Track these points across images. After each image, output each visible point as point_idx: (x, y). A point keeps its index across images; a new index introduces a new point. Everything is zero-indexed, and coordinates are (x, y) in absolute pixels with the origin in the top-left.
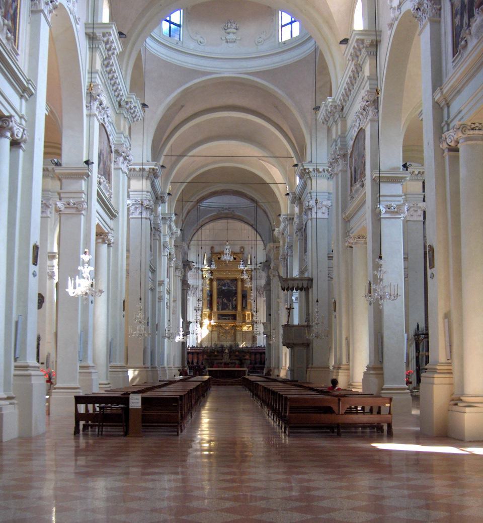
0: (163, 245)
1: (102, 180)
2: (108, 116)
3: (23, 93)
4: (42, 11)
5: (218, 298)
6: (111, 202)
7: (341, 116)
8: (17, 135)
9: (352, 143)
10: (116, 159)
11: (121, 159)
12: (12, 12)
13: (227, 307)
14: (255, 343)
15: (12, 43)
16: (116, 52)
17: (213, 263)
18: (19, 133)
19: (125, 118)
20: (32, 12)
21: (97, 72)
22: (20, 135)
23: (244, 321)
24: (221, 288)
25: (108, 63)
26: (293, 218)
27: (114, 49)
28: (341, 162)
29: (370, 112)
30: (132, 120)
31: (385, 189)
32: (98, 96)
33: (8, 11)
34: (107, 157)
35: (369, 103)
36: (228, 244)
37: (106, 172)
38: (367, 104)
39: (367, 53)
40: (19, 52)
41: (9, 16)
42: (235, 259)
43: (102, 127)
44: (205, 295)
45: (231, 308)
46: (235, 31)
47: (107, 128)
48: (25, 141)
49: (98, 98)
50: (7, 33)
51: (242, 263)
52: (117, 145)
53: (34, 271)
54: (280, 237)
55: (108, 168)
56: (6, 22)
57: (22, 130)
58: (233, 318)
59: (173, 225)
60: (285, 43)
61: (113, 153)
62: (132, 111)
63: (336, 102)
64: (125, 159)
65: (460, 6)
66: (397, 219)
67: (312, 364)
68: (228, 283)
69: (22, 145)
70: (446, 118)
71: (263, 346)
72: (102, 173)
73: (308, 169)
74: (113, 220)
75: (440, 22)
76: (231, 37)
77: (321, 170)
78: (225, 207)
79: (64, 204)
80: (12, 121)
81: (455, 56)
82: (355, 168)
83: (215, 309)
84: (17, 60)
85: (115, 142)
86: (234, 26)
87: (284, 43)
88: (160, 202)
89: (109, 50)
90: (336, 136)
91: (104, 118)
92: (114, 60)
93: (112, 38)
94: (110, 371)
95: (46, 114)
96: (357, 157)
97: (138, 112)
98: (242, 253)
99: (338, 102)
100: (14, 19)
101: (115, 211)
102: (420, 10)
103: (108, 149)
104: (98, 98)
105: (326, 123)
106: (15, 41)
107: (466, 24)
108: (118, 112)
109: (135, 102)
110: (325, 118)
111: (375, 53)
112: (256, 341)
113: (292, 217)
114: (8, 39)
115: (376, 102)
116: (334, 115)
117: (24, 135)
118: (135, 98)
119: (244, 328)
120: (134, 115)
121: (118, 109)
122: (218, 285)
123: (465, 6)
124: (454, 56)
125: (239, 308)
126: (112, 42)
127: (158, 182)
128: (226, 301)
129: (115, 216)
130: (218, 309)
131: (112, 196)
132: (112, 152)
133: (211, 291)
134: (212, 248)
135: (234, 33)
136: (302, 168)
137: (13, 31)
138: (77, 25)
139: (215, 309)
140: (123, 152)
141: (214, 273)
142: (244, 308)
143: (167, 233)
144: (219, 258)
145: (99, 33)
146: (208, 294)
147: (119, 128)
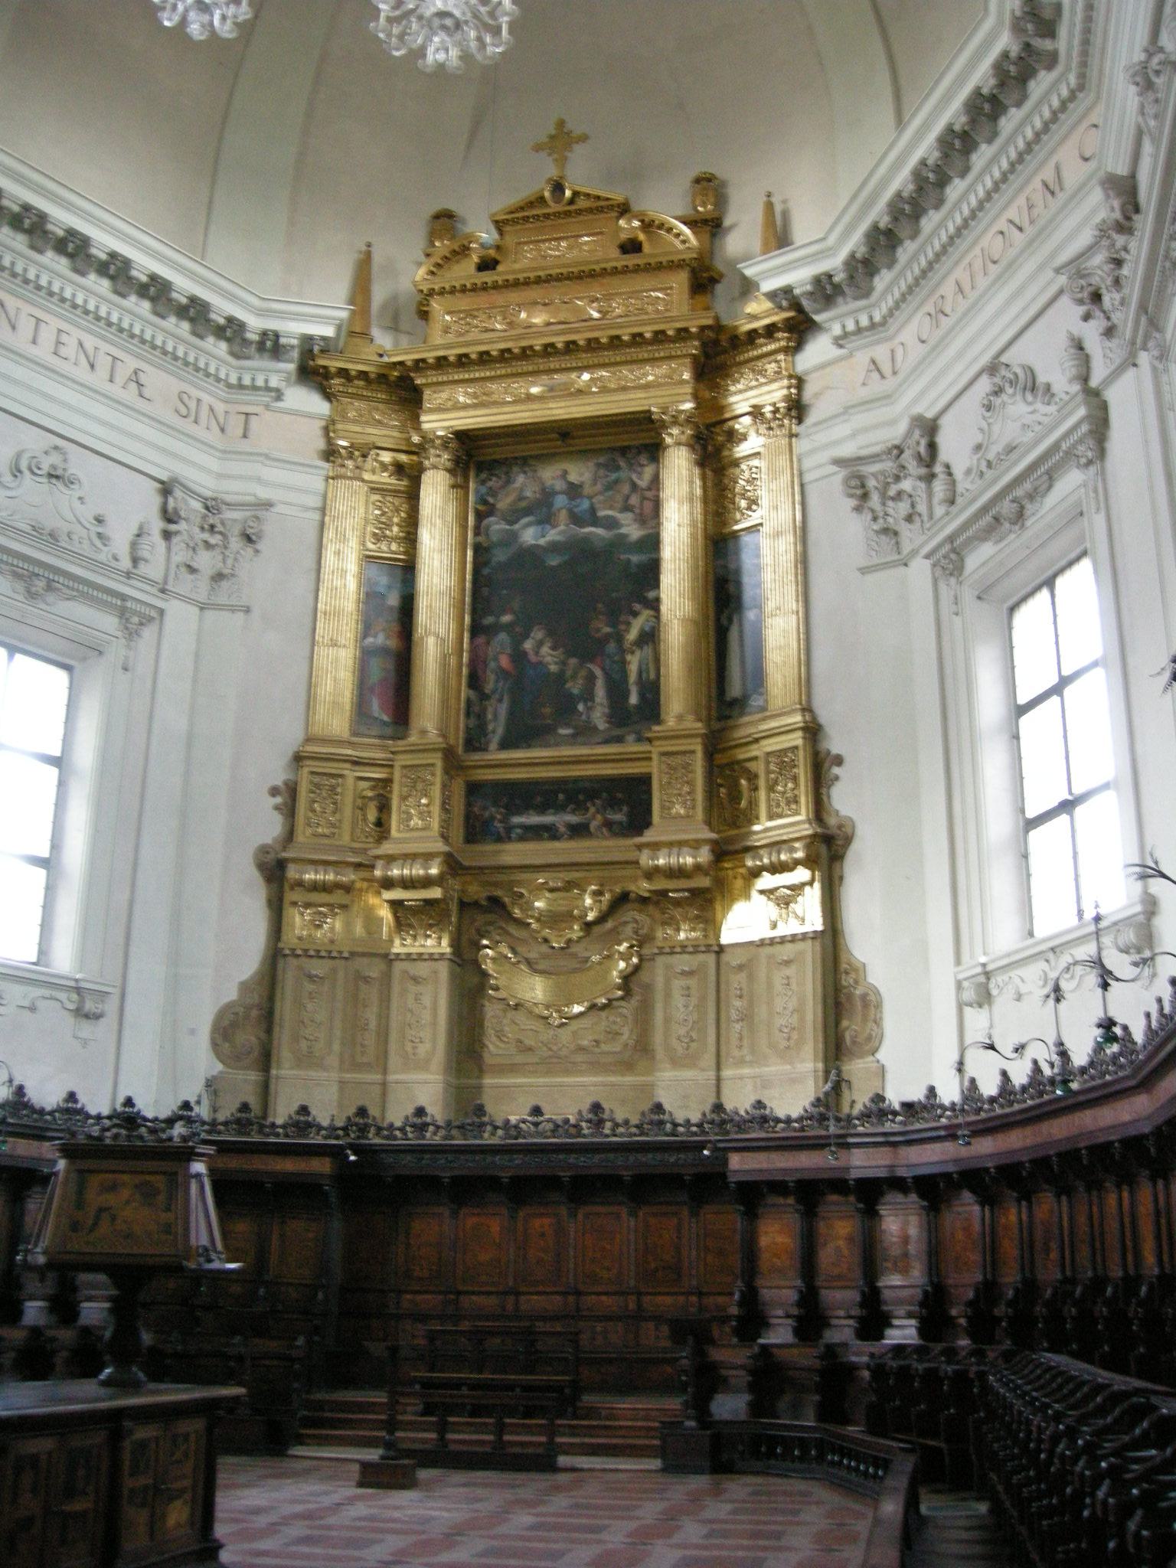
5: (476, 630)
13: (566, 708)
14: (855, 1068)
24: (514, 536)
45: (599, 717)
58: (619, 817)
68: (574, 491)
71: (950, 1093)
112: (872, 1044)
128: (549, 657)
141: (430, 398)
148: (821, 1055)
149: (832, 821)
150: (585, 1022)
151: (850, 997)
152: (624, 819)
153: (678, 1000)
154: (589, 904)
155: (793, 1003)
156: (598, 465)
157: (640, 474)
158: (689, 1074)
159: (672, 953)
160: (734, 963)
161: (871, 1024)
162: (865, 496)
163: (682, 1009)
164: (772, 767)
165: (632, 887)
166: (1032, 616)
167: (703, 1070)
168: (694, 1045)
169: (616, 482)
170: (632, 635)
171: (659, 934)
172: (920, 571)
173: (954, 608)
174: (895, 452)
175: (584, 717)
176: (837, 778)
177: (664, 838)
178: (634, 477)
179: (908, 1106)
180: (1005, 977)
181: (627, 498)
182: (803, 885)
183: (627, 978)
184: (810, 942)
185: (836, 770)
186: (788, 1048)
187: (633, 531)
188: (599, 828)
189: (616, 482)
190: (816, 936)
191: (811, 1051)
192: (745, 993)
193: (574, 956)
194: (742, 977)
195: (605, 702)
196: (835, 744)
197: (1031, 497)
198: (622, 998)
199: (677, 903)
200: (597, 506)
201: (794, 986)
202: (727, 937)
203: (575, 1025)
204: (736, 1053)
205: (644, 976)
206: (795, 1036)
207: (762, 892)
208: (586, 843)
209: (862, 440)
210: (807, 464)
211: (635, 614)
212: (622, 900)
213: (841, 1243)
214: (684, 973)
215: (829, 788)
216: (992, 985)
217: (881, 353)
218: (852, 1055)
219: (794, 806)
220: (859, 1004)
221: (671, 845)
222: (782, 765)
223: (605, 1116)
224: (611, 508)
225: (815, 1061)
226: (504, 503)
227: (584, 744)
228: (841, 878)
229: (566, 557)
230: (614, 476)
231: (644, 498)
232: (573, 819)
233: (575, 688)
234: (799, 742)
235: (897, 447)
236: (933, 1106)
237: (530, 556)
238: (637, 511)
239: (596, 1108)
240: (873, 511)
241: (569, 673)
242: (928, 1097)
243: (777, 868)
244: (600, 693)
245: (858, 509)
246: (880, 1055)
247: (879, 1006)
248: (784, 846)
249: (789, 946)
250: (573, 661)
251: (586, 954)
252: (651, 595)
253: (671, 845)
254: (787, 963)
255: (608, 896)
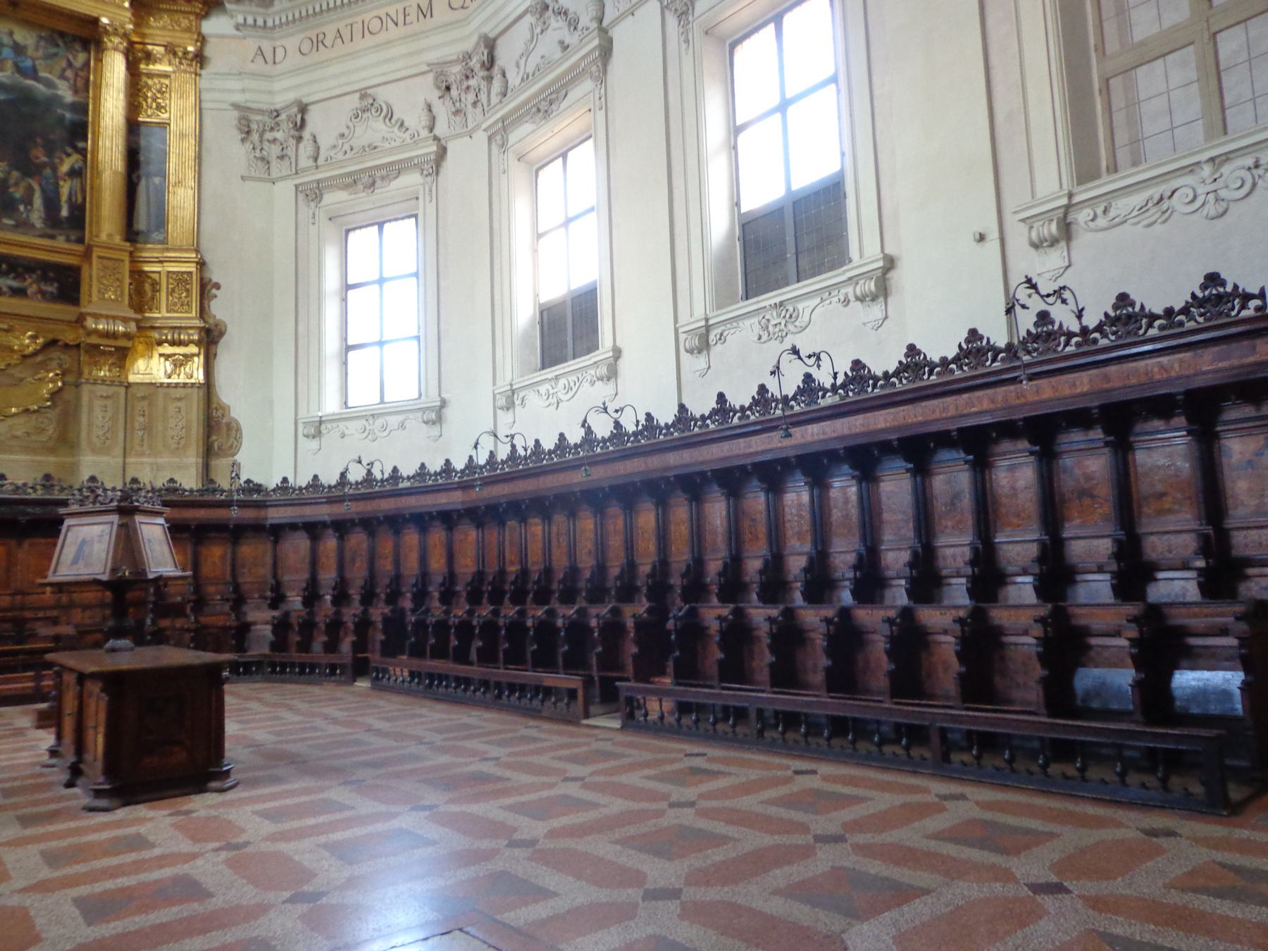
58: (51, 288)
68: (19, 49)
112: (233, 450)
119: (141, 364)
148: (201, 455)
149: (211, 321)
150: (21, 420)
151: (218, 423)
152: (55, 291)
153: (98, 413)
154: (26, 341)
155: (183, 423)
156: (41, 37)
157: (75, 57)
158: (105, 459)
159: (95, 384)
160: (139, 395)
161: (232, 440)
162: (248, 133)
163: (100, 419)
164: (171, 281)
165: (60, 337)
166: (362, 240)
167: (114, 457)
168: (108, 442)
169: (55, 55)
170: (65, 168)
171: (86, 371)
172: (285, 190)
173: (312, 220)
174: (275, 114)
175: (24, 215)
176: (216, 296)
177: (104, 312)
178: (71, 57)
180: (335, 425)
181: (64, 70)
182: (193, 355)
183: (55, 395)
184: (196, 390)
185: (214, 291)
186: (177, 449)
188: (36, 293)
189: (55, 55)
190: (200, 386)
191: (195, 453)
192: (147, 413)
193: (12, 376)
194: (146, 403)
195: (42, 209)
196: (215, 275)
197: (383, 178)
198: (49, 407)
199: (104, 353)
200: (38, 67)
201: (183, 413)
202: (132, 378)
203: (10, 421)
204: (138, 448)
205: (68, 395)
206: (183, 442)
207: (161, 355)
208: (24, 302)
209: (248, 96)
210: (205, 96)
211: (68, 155)
212: (52, 343)
213: (216, 560)
214: (102, 397)
215: (210, 301)
216: (323, 427)
217: (267, 46)
218: (218, 456)
219: (186, 307)
220: (224, 429)
221: (107, 317)
222: (179, 281)
223: (55, 483)
224: (50, 73)
225: (197, 457)
227: (24, 234)
228: (215, 355)
229: (11, 97)
230: (54, 50)
231: (77, 75)
232: (15, 284)
233: (18, 193)
234: (193, 269)
235: (276, 111)
236: (287, 488)
238: (72, 82)
239: (47, 477)
240: (252, 143)
241: (12, 181)
242: (282, 483)
243: (173, 343)
244: (38, 201)
245: (243, 140)
246: (236, 457)
247: (239, 430)
248: (183, 331)
249: (180, 390)
250: (15, 174)
251: (20, 375)
252: (81, 145)
253: (107, 317)
254: (179, 399)
255: (40, 341)
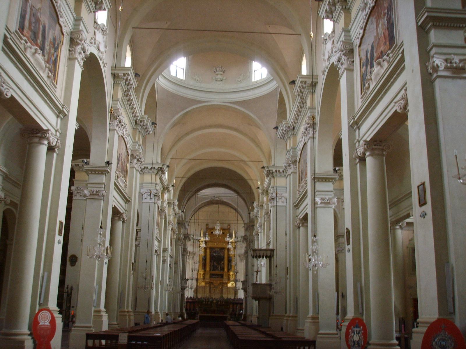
0: (168, 222)
1: (119, 176)
2: (126, 131)
3: (59, 114)
4: (76, 58)
5: (210, 261)
6: (126, 191)
7: (293, 134)
8: (52, 143)
9: (299, 152)
10: (132, 160)
11: (136, 160)
12: (53, 58)
14: (236, 296)
15: (52, 80)
16: (134, 86)
17: (207, 236)
18: (54, 141)
19: (140, 132)
20: (69, 59)
21: (118, 100)
22: (54, 144)
23: (229, 280)
24: (213, 255)
25: (128, 94)
26: (263, 205)
27: (131, 84)
28: (292, 166)
29: (310, 132)
30: (145, 133)
31: (320, 186)
32: (119, 116)
33: (51, 58)
34: (124, 159)
35: (309, 125)
36: (218, 222)
37: (123, 171)
38: (308, 126)
39: (308, 91)
40: (57, 86)
41: (51, 61)
42: (223, 233)
43: (121, 137)
44: (201, 260)
45: (219, 269)
46: (222, 73)
47: (125, 139)
48: (58, 147)
49: (118, 118)
50: (48, 73)
51: (228, 236)
52: (133, 150)
53: (59, 240)
54: (255, 218)
55: (125, 167)
56: (48, 65)
57: (56, 140)
59: (176, 208)
60: (256, 82)
61: (130, 157)
62: (145, 127)
63: (289, 124)
64: (138, 160)
65: (365, 60)
66: (329, 208)
67: (273, 313)
68: (218, 251)
69: (56, 150)
70: (357, 137)
71: (242, 298)
72: (120, 170)
73: (272, 170)
74: (127, 204)
75: (353, 70)
76: (219, 77)
77: (281, 171)
78: (216, 196)
79: (90, 192)
80: (48, 134)
81: (363, 94)
82: (302, 171)
83: (208, 269)
84: (56, 92)
85: (131, 149)
86: (221, 69)
87: (256, 82)
88: (166, 191)
89: (128, 85)
90: (289, 148)
91: (123, 132)
92: (132, 92)
93: (130, 77)
94: (119, 315)
95: (76, 129)
96: (303, 163)
97: (149, 128)
98: (229, 229)
99: (290, 124)
100: (55, 63)
101: (129, 198)
102: (340, 62)
103: (126, 154)
104: (118, 118)
105: (282, 138)
106: (55, 79)
107: (369, 72)
108: (134, 127)
109: (147, 121)
110: (281, 135)
111: (312, 91)
113: (262, 204)
114: (49, 77)
115: (314, 124)
116: (288, 133)
117: (58, 144)
118: (147, 119)
120: (146, 130)
121: (135, 126)
122: (211, 252)
123: (368, 60)
124: (362, 93)
125: (226, 270)
126: (130, 80)
127: (166, 176)
128: (216, 264)
129: (129, 201)
130: (210, 270)
131: (127, 187)
132: (128, 156)
133: (205, 256)
134: (207, 225)
135: (221, 75)
136: (267, 169)
137: (54, 71)
138: (105, 68)
139: (208, 269)
140: (137, 156)
142: (229, 270)
143: (171, 213)
144: (212, 233)
145: (121, 73)
146: (203, 259)
147: (135, 138)
179: (240, 299)
187: (222, 255)
226: (213, 251)
233: (218, 267)
237: (214, 256)
244: (220, 268)
